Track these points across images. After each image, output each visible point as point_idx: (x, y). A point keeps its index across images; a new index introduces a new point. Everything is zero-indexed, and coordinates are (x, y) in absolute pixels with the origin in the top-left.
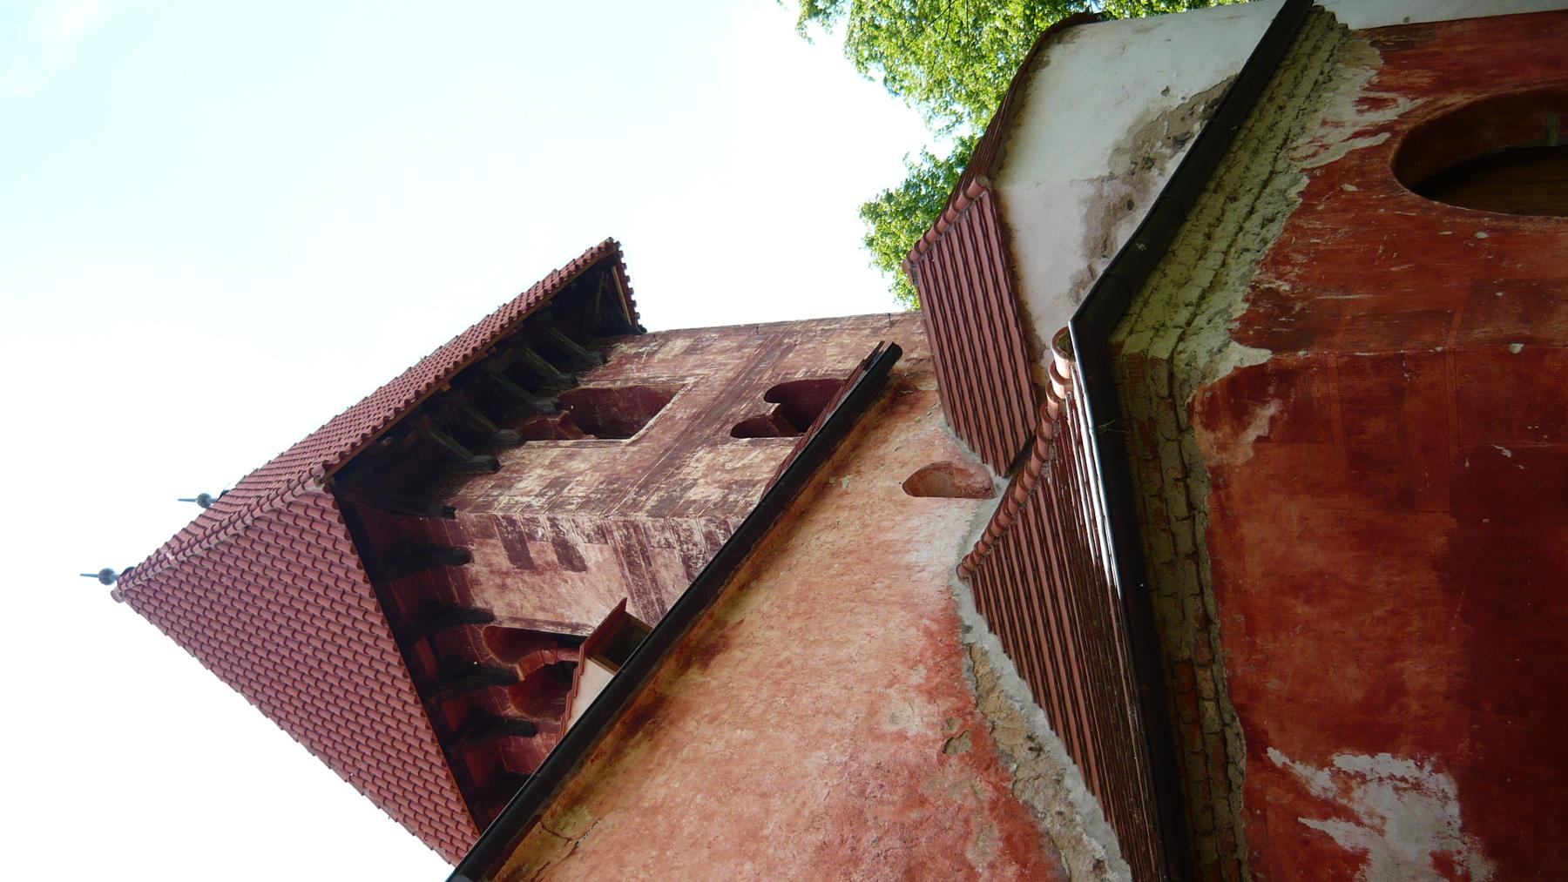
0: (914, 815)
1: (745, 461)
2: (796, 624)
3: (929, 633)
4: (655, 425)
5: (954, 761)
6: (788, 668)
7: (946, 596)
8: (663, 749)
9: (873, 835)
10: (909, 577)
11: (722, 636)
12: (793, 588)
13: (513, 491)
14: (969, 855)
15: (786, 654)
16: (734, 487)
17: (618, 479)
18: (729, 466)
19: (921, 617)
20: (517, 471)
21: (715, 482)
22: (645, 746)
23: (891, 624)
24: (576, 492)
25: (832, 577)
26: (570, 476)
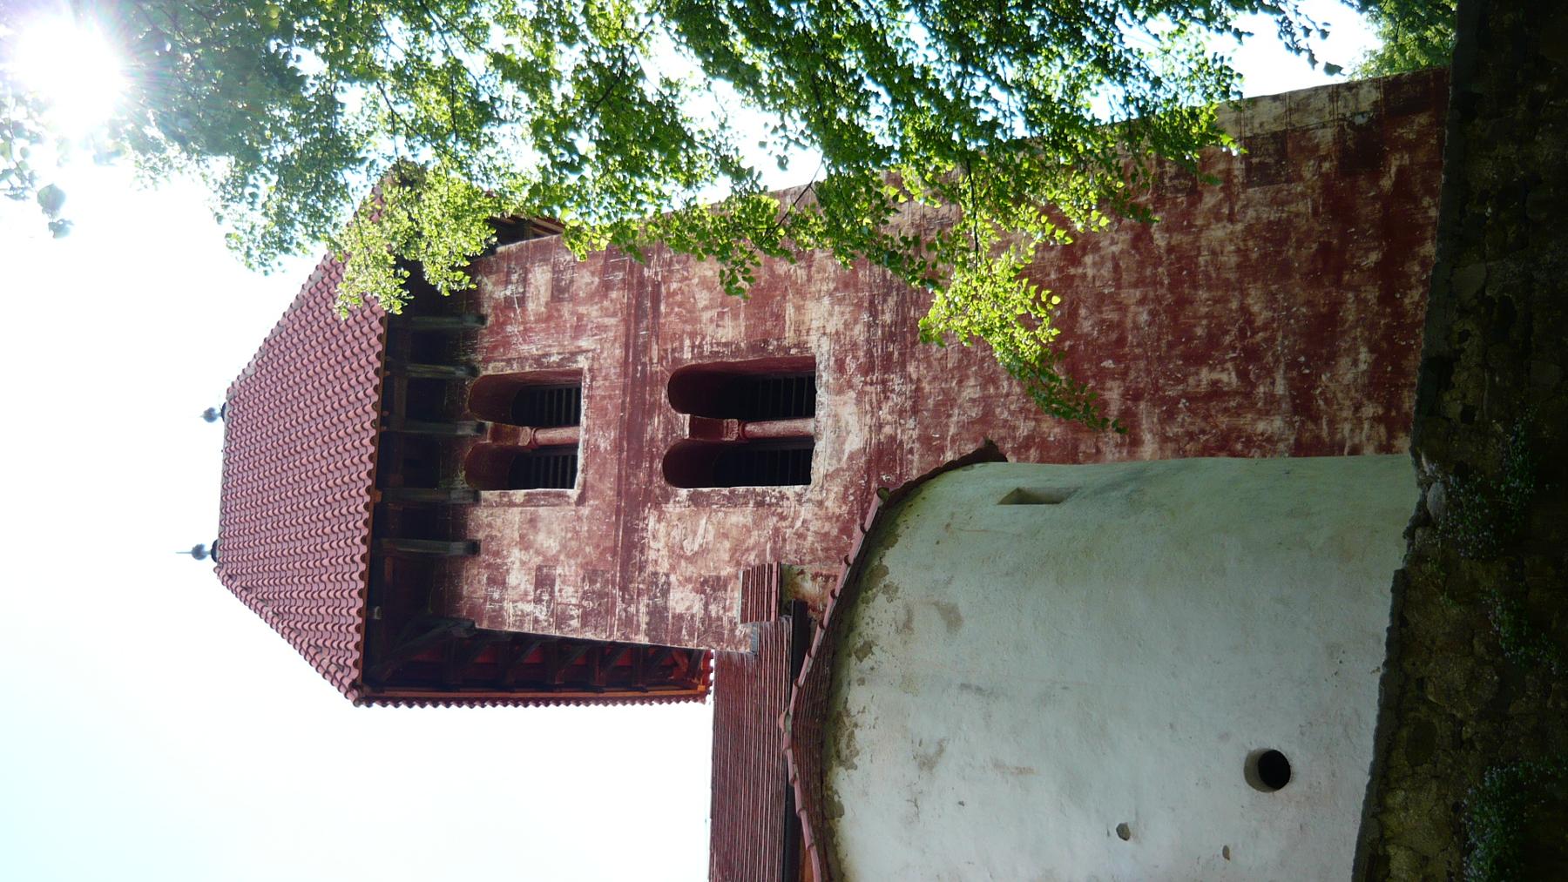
1: (699, 540)
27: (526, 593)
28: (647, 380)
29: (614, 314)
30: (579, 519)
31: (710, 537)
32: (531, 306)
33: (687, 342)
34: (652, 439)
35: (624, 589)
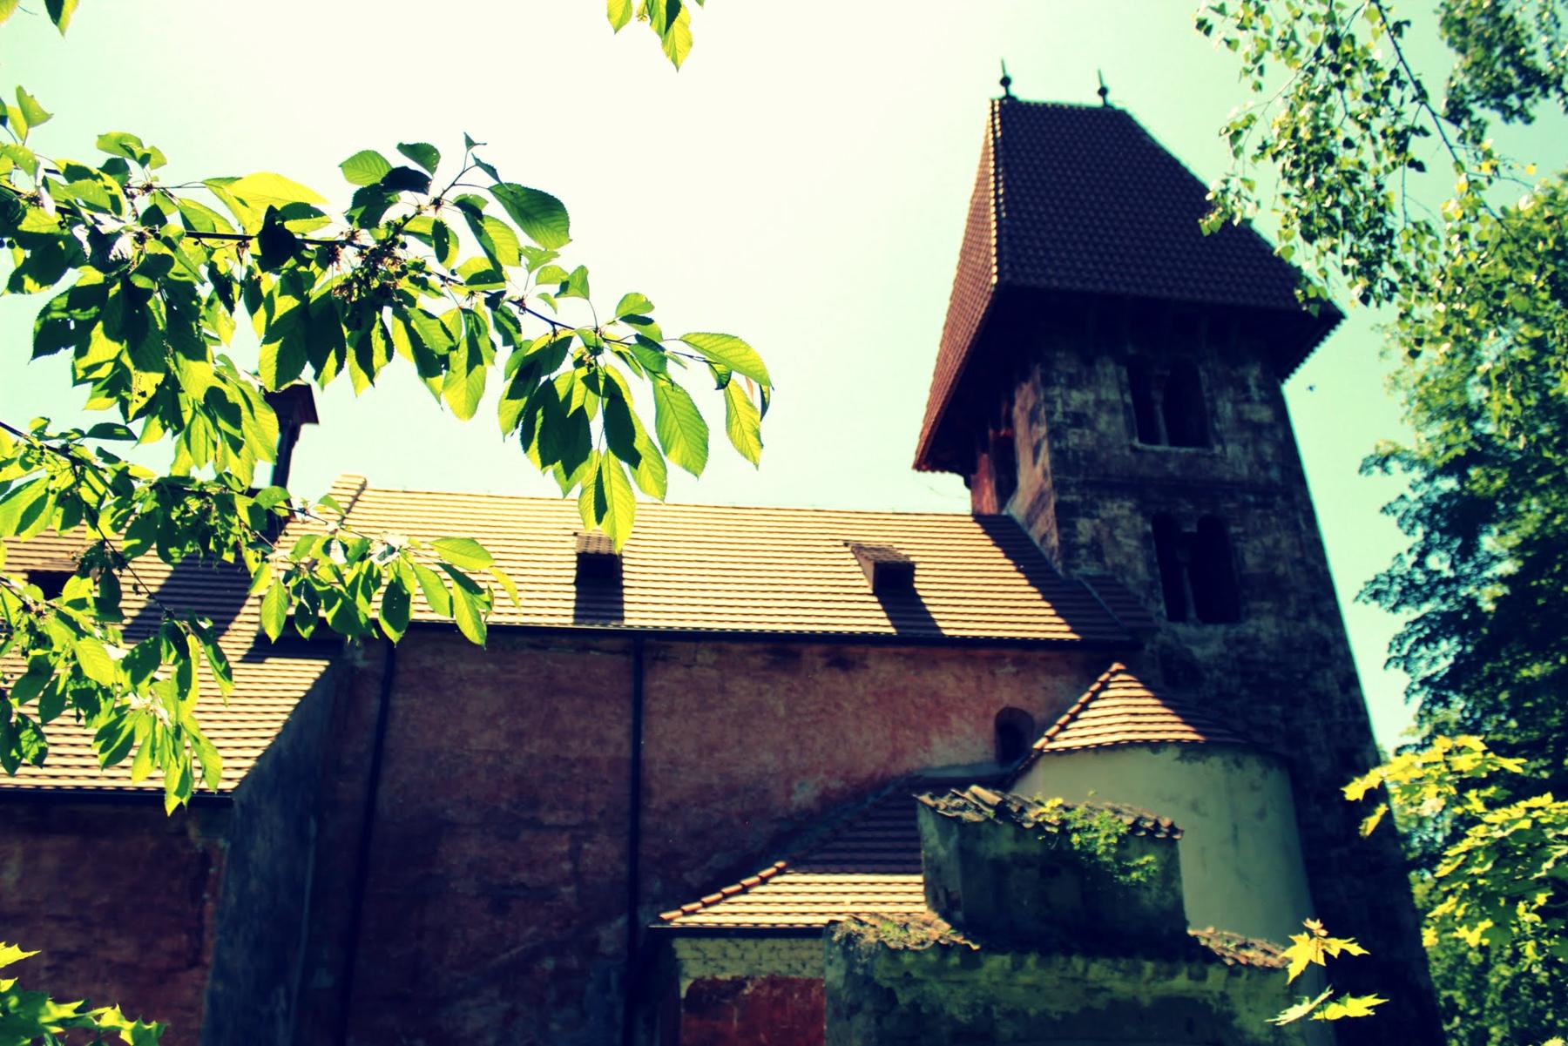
30: (1122, 447)
31: (1126, 549)
35: (1085, 483)
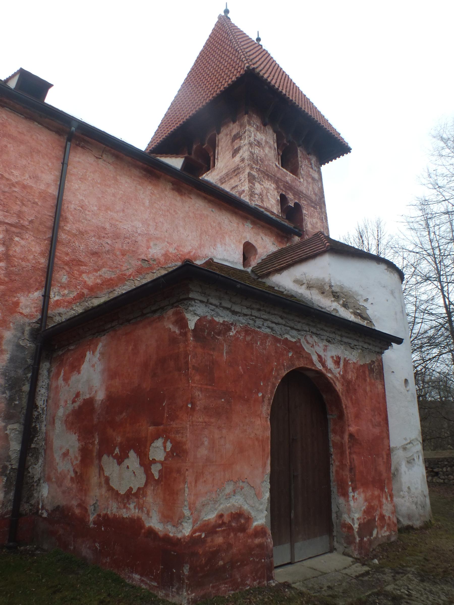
0: (118, 253)
1: (271, 199)
2: (191, 214)
3: (190, 252)
4: (283, 171)
5: (140, 262)
6: (174, 213)
7: (204, 256)
8: (140, 180)
9: (109, 242)
10: (211, 245)
11: (185, 194)
12: (205, 212)
13: (255, 131)
14: (104, 269)
15: (179, 212)
16: (261, 196)
17: (262, 162)
18: (269, 194)
19: (196, 250)
20: (264, 132)
21: (262, 191)
22: (140, 175)
23: (192, 241)
24: (256, 150)
25: (210, 224)
26: (263, 148)
27: (256, 137)
28: (299, 199)
29: (311, 194)
31: (271, 202)
32: (311, 170)
33: (307, 213)
34: (289, 194)
